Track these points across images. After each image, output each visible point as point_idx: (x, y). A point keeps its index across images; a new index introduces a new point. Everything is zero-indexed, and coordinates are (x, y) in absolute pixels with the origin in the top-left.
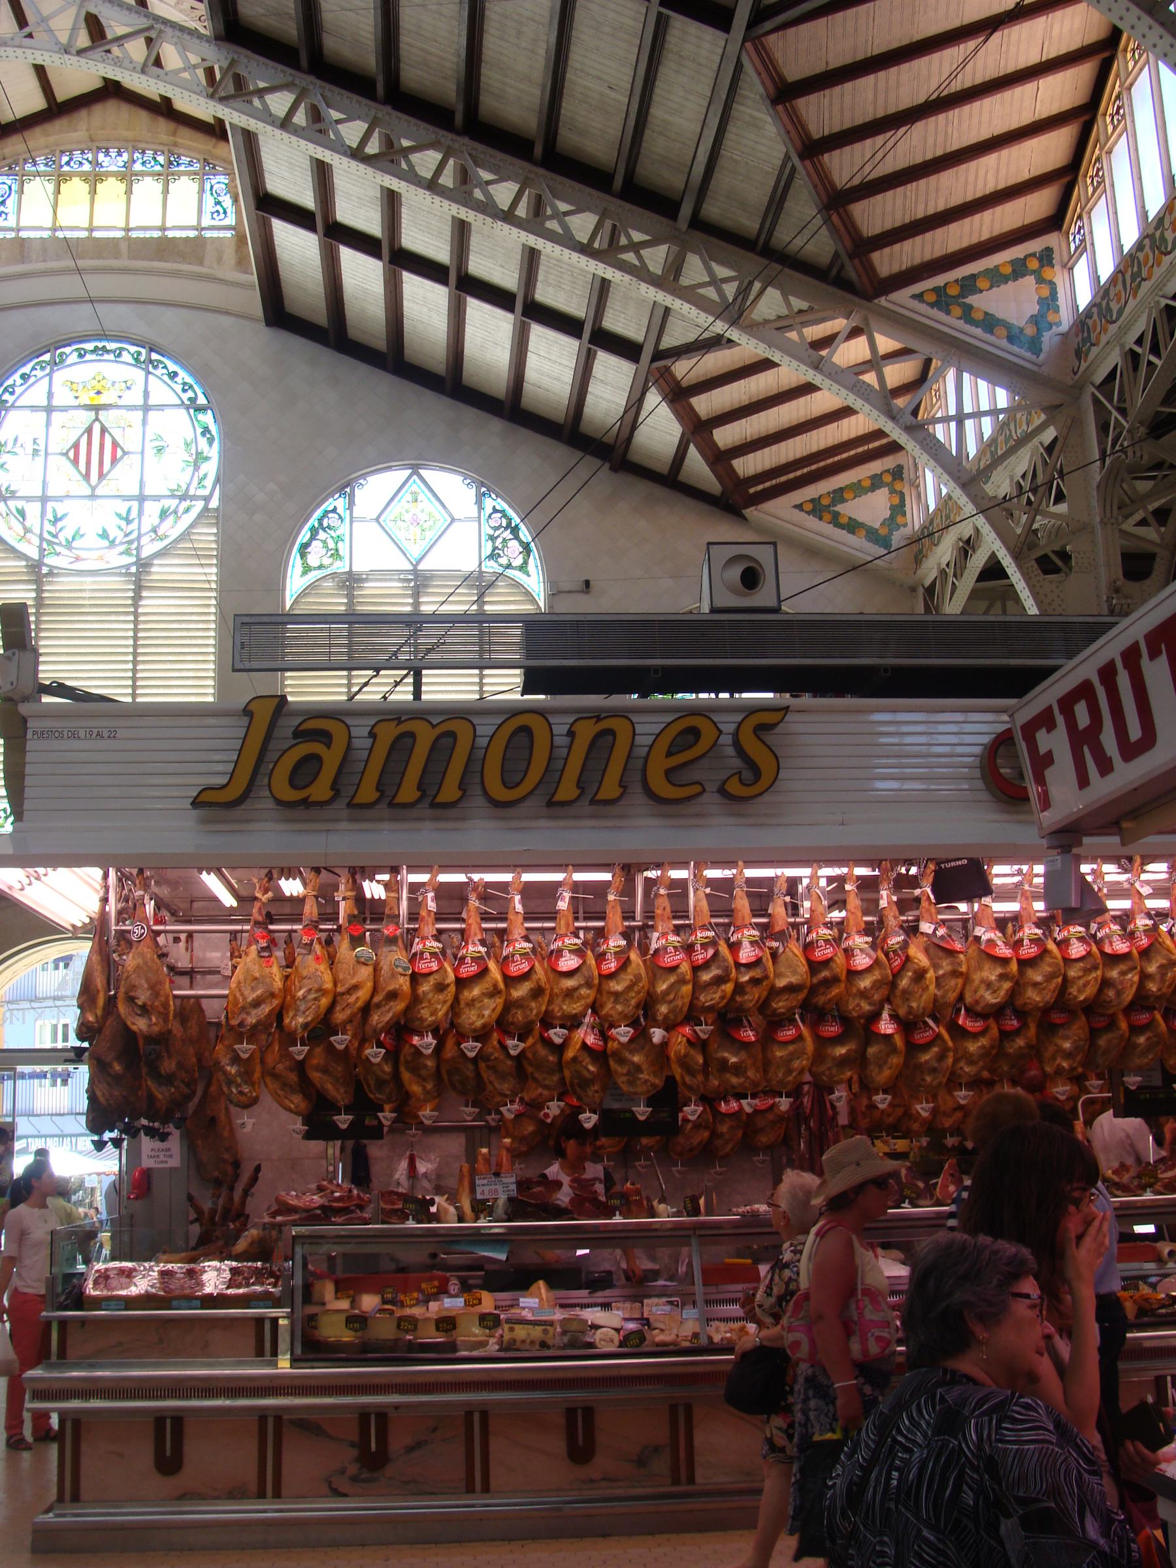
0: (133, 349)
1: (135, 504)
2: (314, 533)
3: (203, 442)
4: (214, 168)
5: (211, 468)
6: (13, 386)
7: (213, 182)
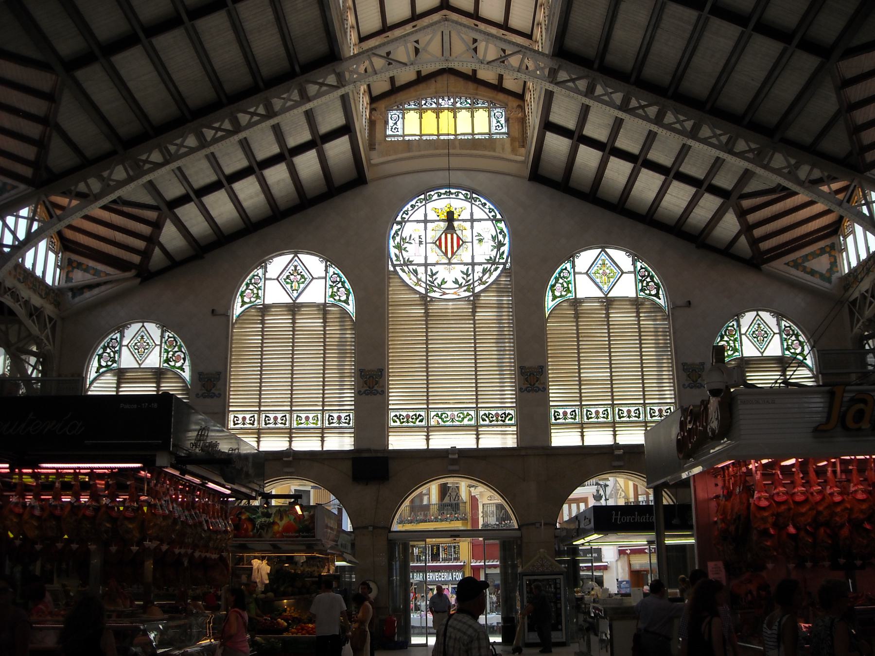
0: (464, 192)
1: (470, 267)
2: (557, 280)
3: (500, 237)
4: (495, 105)
5: (505, 249)
6: (407, 211)
7: (495, 111)
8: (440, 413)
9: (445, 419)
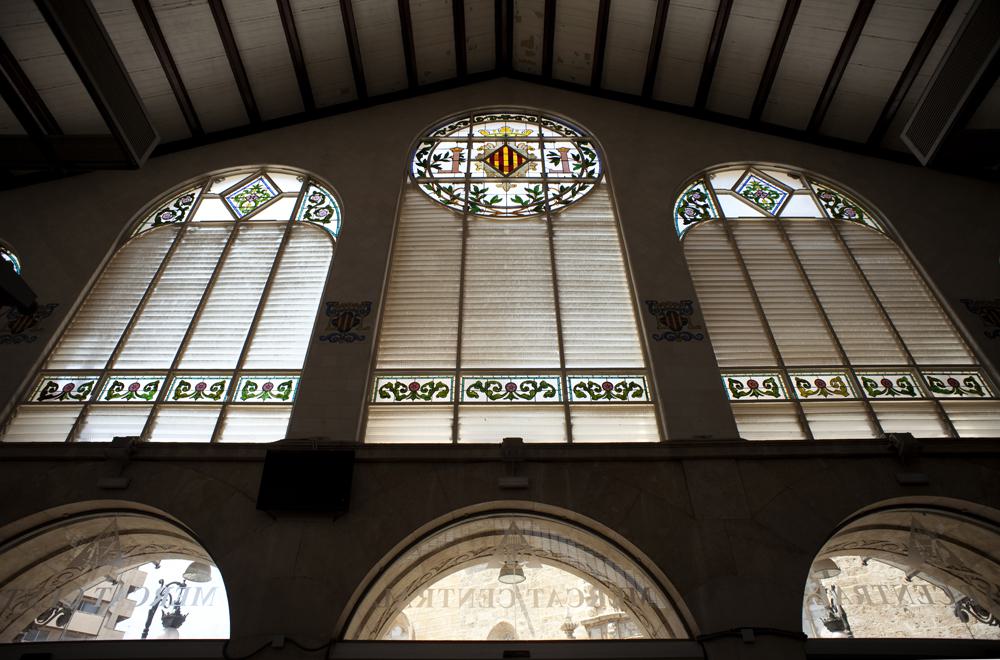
5: (597, 168)
8: (484, 382)
9: (494, 393)
